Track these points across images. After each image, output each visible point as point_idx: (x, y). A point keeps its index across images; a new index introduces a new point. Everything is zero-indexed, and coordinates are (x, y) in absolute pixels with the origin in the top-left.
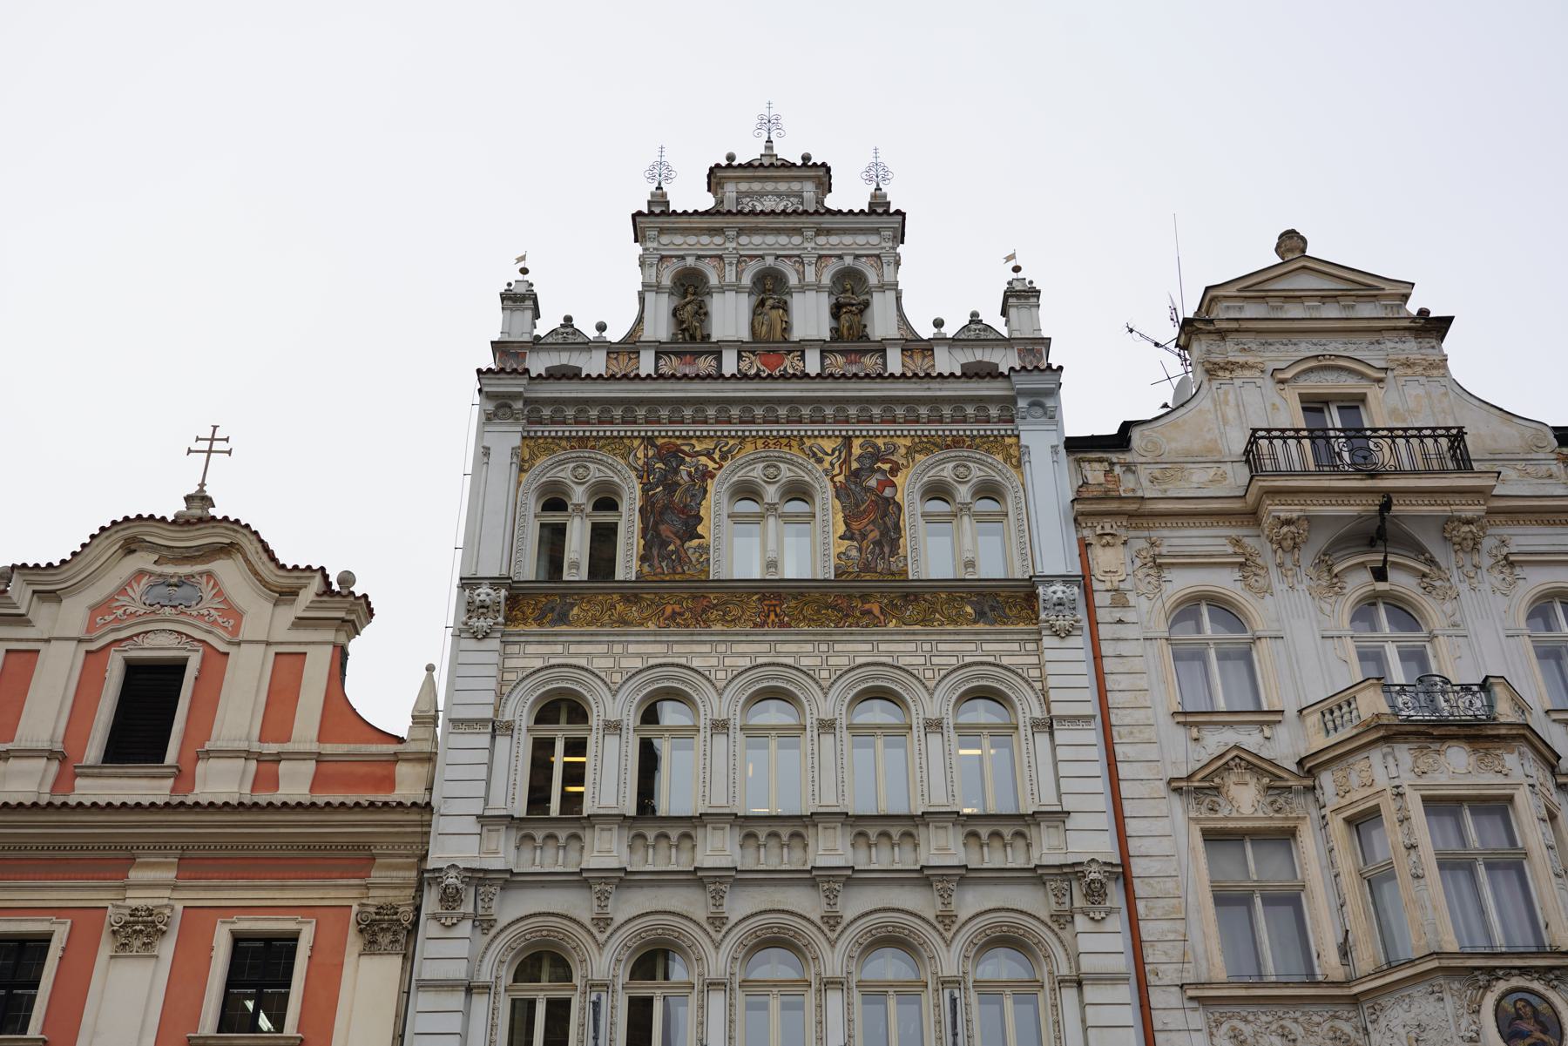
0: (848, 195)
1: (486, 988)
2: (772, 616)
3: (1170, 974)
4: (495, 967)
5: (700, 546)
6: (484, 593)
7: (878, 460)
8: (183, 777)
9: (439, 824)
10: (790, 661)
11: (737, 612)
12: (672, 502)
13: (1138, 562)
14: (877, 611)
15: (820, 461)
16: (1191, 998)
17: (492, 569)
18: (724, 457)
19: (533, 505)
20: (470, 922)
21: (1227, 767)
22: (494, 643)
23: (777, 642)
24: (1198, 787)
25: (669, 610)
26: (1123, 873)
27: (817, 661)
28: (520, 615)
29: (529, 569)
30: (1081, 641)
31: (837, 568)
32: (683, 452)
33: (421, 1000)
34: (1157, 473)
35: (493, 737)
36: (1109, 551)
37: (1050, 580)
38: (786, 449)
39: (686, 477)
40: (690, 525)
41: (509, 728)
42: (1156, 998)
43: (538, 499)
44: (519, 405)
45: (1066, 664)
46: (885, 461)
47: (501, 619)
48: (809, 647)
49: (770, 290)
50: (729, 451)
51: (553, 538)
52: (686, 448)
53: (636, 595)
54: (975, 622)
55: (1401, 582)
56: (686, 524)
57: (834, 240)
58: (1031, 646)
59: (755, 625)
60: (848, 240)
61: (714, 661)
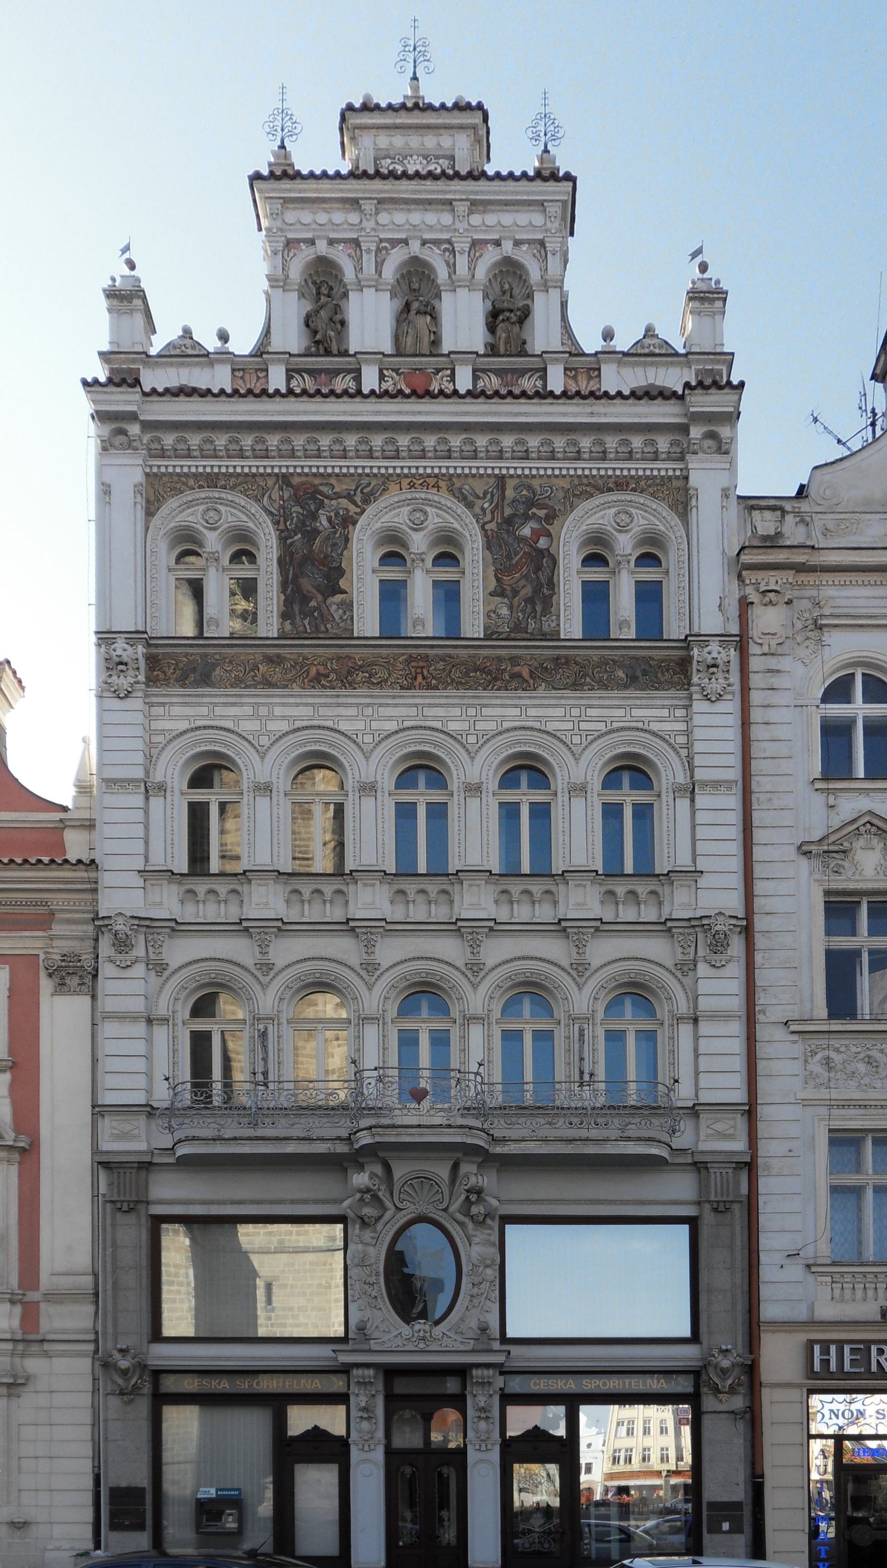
0: (512, 152)
1: (165, 1020)
2: (420, 678)
3: (776, 1014)
4: (173, 1001)
5: (342, 603)
6: (121, 648)
7: (533, 505)
9: (106, 879)
10: (438, 725)
11: (382, 674)
12: (311, 551)
13: (799, 625)
14: (525, 673)
15: (470, 506)
16: (793, 1032)
17: (126, 621)
18: (367, 501)
19: (165, 556)
20: (143, 965)
21: (857, 833)
22: (136, 703)
23: (424, 705)
24: (827, 851)
25: (313, 671)
27: (465, 725)
28: (162, 676)
30: (731, 706)
31: (486, 628)
32: (321, 493)
33: (109, 1029)
34: (831, 526)
35: (147, 798)
36: (771, 611)
37: (703, 640)
38: (435, 490)
39: (325, 523)
40: (333, 578)
41: (162, 788)
42: (762, 1033)
43: (171, 547)
44: (134, 429)
46: (541, 507)
47: (142, 678)
48: (457, 711)
49: (417, 296)
50: (372, 493)
52: (324, 489)
53: (279, 656)
54: (626, 687)
56: (327, 577)
57: (491, 219)
58: (680, 713)
59: (402, 688)
60: (507, 219)
61: (360, 725)
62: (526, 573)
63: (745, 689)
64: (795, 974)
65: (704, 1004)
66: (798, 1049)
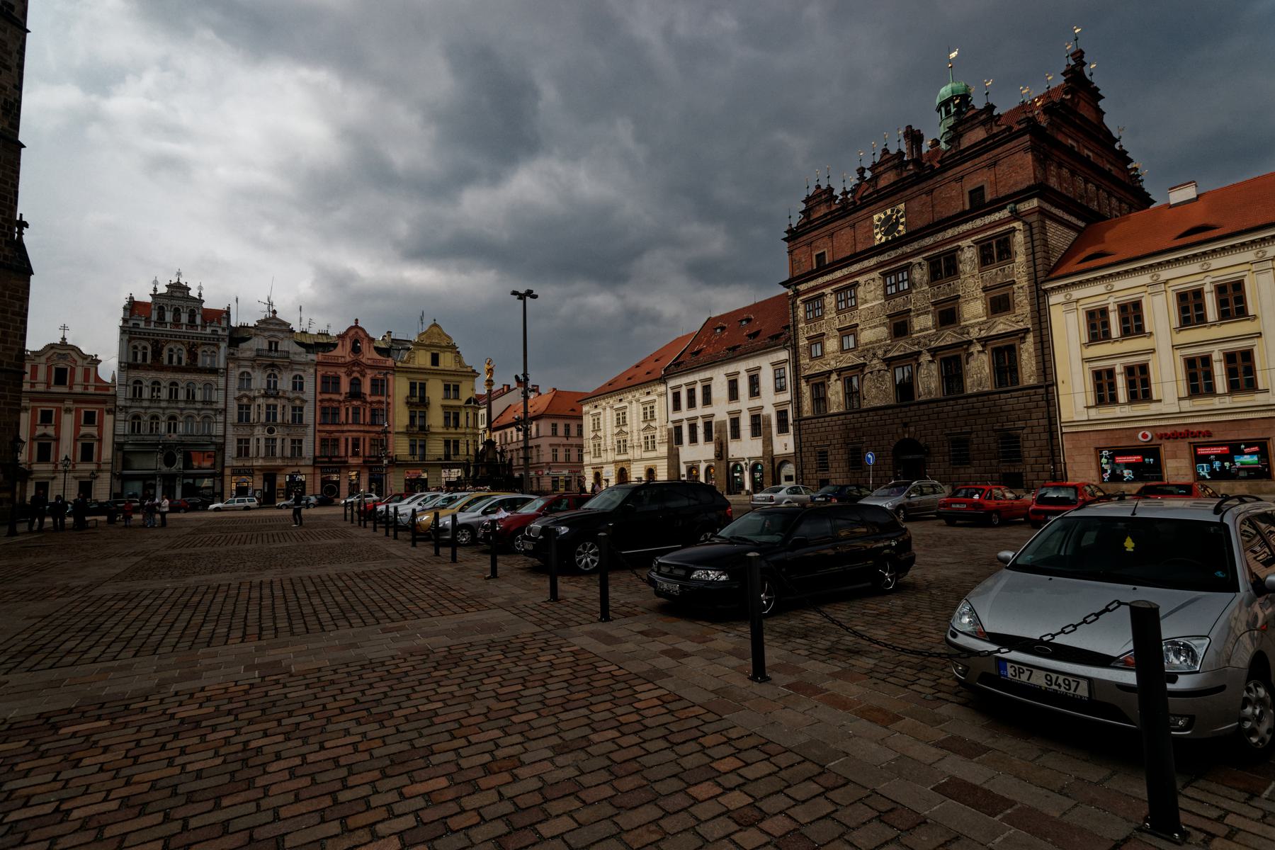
8: (71, 388)
24: (239, 399)
26: (225, 410)
29: (131, 360)
45: (222, 381)
51: (135, 354)
62: (193, 356)
64: (233, 414)
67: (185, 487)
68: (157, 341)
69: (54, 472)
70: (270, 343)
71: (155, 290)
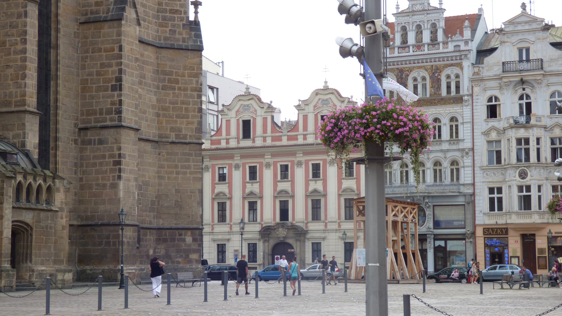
24: (486, 133)
26: (473, 149)
30: (470, 107)
42: (475, 169)
49: (419, 30)
55: (528, 91)
62: (436, 82)
63: (473, 103)
64: (482, 157)
65: (465, 164)
66: (482, 172)
67: (437, 250)
68: (401, 71)
69: (325, 231)
70: (520, 50)
71: (398, 7)
